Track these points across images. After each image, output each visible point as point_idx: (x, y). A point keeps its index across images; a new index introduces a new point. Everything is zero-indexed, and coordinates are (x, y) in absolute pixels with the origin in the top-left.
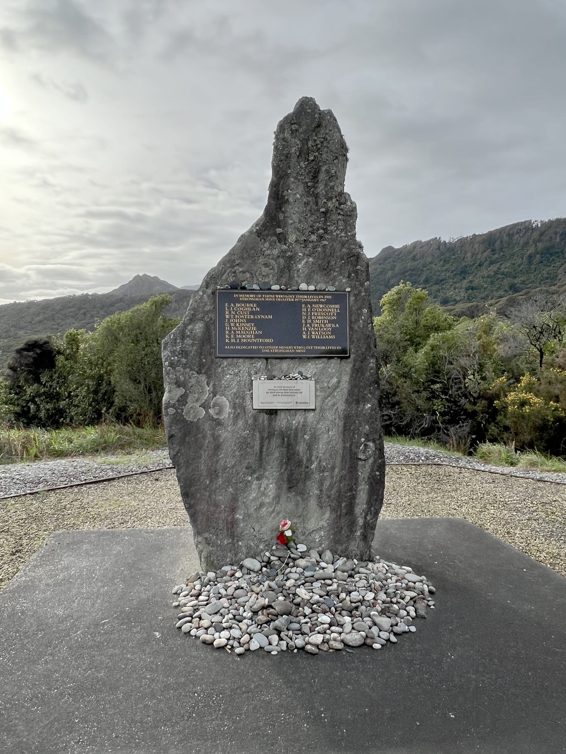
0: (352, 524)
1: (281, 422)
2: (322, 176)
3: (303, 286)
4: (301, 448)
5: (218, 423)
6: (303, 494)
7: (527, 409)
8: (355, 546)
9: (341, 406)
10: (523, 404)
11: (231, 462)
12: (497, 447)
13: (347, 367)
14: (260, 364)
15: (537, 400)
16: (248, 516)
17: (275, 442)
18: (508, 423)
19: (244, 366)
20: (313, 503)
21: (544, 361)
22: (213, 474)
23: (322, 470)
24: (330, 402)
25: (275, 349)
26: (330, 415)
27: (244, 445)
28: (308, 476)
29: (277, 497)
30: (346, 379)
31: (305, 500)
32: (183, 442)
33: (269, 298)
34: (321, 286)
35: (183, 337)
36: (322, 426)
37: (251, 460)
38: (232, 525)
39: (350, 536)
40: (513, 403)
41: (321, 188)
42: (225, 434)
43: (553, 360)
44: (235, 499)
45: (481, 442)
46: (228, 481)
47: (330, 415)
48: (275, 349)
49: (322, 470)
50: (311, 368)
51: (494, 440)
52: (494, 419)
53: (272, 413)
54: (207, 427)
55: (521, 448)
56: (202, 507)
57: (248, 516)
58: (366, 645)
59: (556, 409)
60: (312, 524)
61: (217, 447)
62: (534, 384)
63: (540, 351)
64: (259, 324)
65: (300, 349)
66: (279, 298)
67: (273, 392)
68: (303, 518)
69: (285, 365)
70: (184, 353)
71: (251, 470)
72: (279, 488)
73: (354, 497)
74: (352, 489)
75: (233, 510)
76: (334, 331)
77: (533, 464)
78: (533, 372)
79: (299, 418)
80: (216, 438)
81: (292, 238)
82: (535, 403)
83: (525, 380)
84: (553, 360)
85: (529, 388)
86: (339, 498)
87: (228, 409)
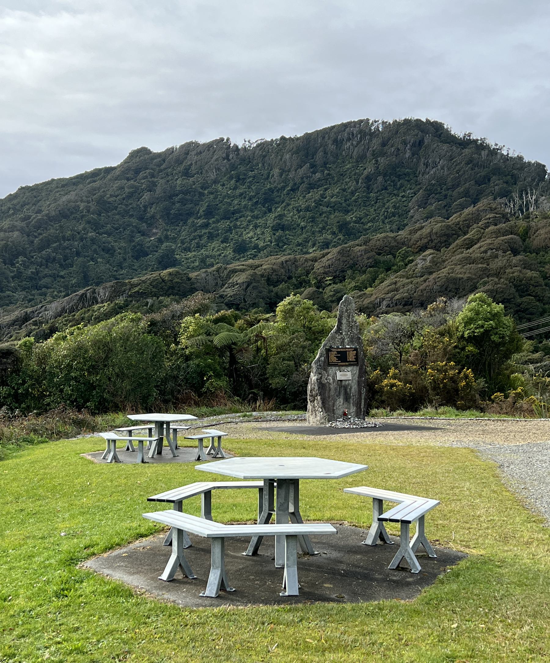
0: (361, 410)
1: (343, 383)
2: (351, 316)
3: (347, 346)
4: (348, 390)
5: (330, 384)
6: (349, 402)
7: (394, 389)
8: (361, 417)
9: (357, 379)
10: (392, 385)
11: (333, 394)
12: (381, 411)
13: (358, 368)
14: (337, 368)
15: (400, 383)
16: (337, 408)
17: (342, 388)
18: (384, 398)
19: (334, 368)
20: (351, 405)
21: (402, 359)
22: (329, 397)
23: (353, 396)
24: (354, 377)
25: (341, 364)
26: (354, 381)
27: (336, 389)
28: (350, 398)
29: (343, 403)
30: (358, 371)
31: (350, 404)
32: (322, 388)
33: (339, 350)
34: (351, 346)
35: (319, 361)
36: (353, 384)
37: (337, 393)
38: (334, 410)
39: (360, 414)
40: (387, 385)
41: (350, 320)
42: (332, 387)
43: (408, 358)
44: (334, 404)
45: (371, 409)
46: (332, 399)
47: (354, 381)
48: (341, 364)
49: (353, 396)
50: (350, 368)
51: (378, 408)
52: (374, 398)
53: (341, 381)
54: (327, 385)
55: (393, 410)
56: (327, 406)
57: (337, 408)
58: (375, 427)
59: (411, 388)
60: (351, 411)
61: (330, 390)
62: (397, 374)
63: (400, 353)
64: (337, 357)
65: (347, 363)
66: (342, 350)
67: (341, 375)
68: (349, 409)
69: (343, 368)
70: (320, 365)
71: (337, 396)
72: (344, 401)
73: (361, 403)
74: (360, 401)
75: (334, 407)
76: (355, 358)
77: (401, 415)
78: (396, 366)
79: (347, 382)
80: (330, 387)
81: (344, 334)
82: (399, 385)
83: (392, 372)
84: (408, 358)
85: (394, 377)
86: (357, 404)
87: (331, 380)
